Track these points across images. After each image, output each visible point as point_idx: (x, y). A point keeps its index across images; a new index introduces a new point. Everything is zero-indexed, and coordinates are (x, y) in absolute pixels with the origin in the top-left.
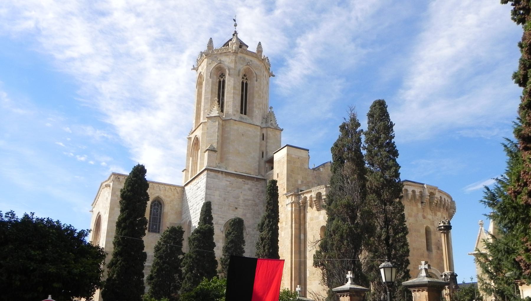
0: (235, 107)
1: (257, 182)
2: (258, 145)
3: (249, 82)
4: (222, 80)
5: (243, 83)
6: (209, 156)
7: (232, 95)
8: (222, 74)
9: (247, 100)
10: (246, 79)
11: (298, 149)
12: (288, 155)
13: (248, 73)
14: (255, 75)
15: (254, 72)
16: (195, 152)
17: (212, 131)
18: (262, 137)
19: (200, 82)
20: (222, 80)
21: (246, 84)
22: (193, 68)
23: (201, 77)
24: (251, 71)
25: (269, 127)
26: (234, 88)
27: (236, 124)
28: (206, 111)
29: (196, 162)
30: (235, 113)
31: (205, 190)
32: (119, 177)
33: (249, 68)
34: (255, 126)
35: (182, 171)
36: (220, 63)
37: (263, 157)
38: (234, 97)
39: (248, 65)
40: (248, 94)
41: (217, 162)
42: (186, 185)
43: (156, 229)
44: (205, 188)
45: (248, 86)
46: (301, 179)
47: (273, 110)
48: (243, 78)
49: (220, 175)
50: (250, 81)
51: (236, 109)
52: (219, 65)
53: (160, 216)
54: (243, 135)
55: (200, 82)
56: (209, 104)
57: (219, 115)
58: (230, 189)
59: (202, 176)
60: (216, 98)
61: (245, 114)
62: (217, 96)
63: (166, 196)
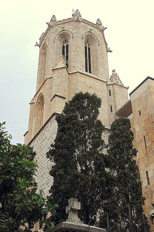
3: (91, 48)
4: (65, 45)
5: (86, 48)
9: (91, 62)
16: (39, 111)
17: (59, 81)
18: (109, 93)
21: (89, 49)
24: (93, 37)
25: (115, 84)
29: (40, 120)
33: (91, 35)
35: (23, 135)
36: (64, 30)
37: (112, 111)
40: (91, 57)
52: (63, 32)
59: (49, 125)
61: (90, 72)
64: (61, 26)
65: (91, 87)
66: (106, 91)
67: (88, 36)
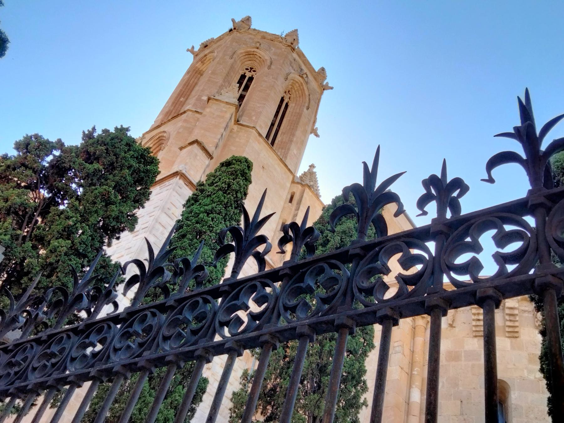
4: (248, 75)
5: (282, 100)
13: (295, 91)
18: (289, 197)
19: (199, 69)
20: (248, 75)
22: (190, 48)
23: (205, 62)
24: (303, 89)
27: (259, 143)
33: (301, 83)
34: (287, 170)
36: (258, 48)
39: (302, 77)
47: (314, 170)
50: (294, 105)
52: (256, 50)
55: (199, 69)
65: (265, 167)
66: (287, 191)
67: (294, 82)
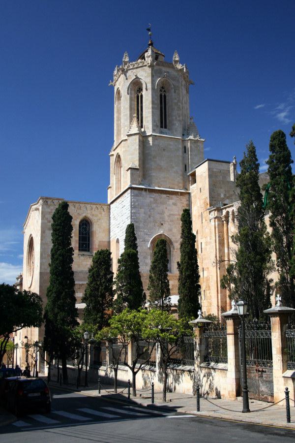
0: (155, 122)
1: (181, 197)
2: (181, 158)
3: (167, 95)
5: (161, 95)
6: (132, 175)
7: (151, 110)
8: (139, 89)
10: (165, 91)
11: (219, 163)
12: (209, 169)
14: (173, 86)
15: (171, 83)
20: (140, 95)
21: (165, 96)
26: (153, 103)
28: (126, 128)
30: (155, 128)
31: (130, 209)
32: (47, 200)
37: (186, 170)
38: (153, 112)
41: (140, 179)
42: (112, 203)
43: (86, 247)
44: (130, 207)
45: (167, 98)
46: (224, 192)
48: (161, 91)
49: (143, 192)
51: (155, 124)
52: (137, 79)
53: (89, 235)
54: (164, 150)
56: (129, 121)
57: (138, 132)
58: (155, 205)
59: (126, 194)
60: (135, 115)
61: (166, 127)
62: (136, 111)
63: (93, 215)
64: (134, 71)
